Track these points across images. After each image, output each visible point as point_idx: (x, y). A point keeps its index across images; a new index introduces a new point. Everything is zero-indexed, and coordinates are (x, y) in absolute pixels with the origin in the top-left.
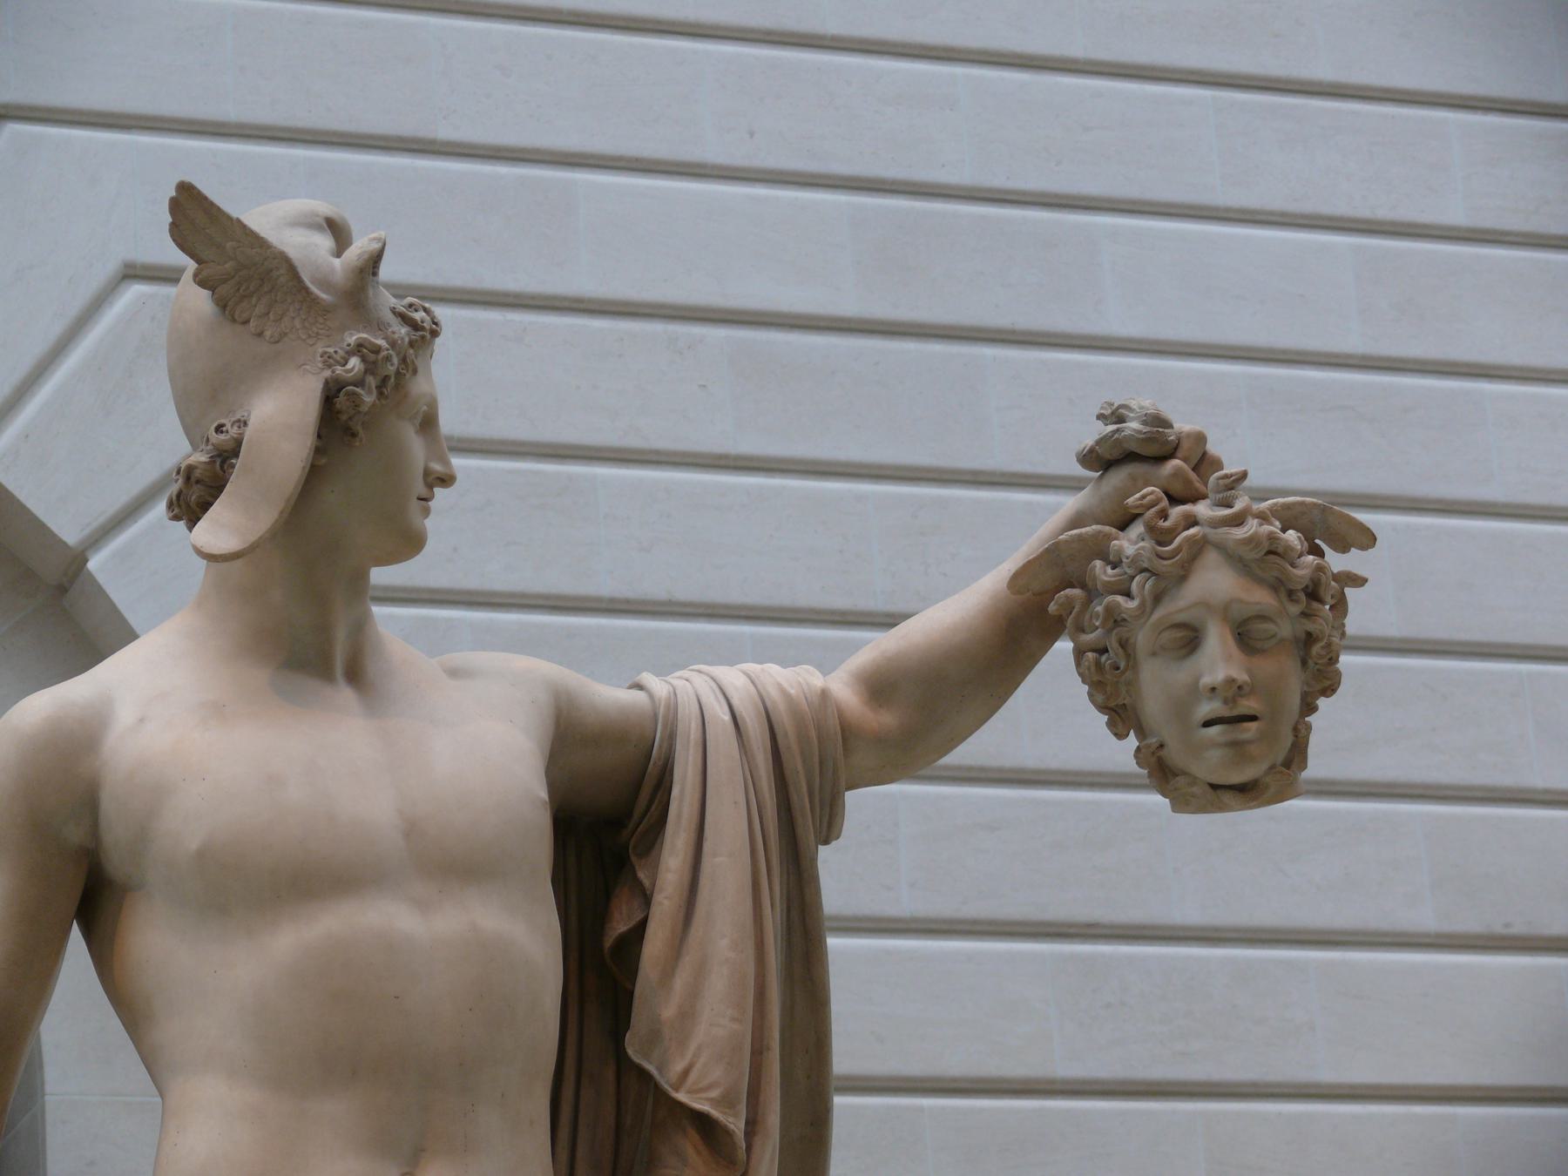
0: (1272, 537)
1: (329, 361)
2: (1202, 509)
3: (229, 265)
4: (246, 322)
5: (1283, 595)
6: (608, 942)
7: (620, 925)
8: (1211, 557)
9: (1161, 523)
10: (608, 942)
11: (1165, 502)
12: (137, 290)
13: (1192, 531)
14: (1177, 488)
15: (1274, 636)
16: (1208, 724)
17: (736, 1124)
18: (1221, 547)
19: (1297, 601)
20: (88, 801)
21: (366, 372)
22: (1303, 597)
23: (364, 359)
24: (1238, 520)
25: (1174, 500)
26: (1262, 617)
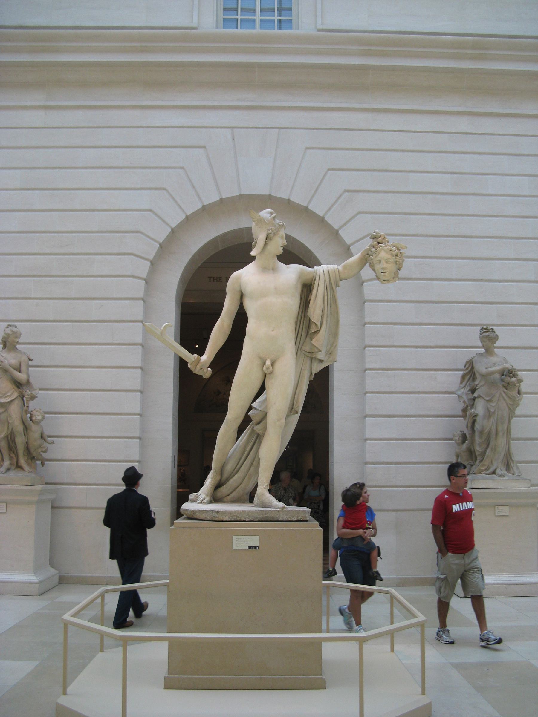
0: (391, 248)
1: (268, 230)
2: (382, 245)
3: (257, 219)
4: (259, 226)
5: (392, 256)
6: (308, 300)
7: (309, 299)
8: (383, 251)
9: (377, 247)
10: (308, 300)
11: (377, 244)
12: (347, 193)
13: (381, 247)
14: (380, 242)
15: (391, 261)
16: (382, 273)
17: (319, 324)
18: (383, 249)
19: (394, 257)
20: (240, 286)
21: (272, 232)
22: (395, 256)
23: (272, 230)
24: (386, 246)
25: (379, 243)
26: (389, 259)
